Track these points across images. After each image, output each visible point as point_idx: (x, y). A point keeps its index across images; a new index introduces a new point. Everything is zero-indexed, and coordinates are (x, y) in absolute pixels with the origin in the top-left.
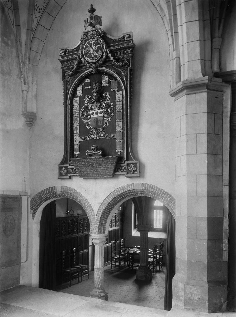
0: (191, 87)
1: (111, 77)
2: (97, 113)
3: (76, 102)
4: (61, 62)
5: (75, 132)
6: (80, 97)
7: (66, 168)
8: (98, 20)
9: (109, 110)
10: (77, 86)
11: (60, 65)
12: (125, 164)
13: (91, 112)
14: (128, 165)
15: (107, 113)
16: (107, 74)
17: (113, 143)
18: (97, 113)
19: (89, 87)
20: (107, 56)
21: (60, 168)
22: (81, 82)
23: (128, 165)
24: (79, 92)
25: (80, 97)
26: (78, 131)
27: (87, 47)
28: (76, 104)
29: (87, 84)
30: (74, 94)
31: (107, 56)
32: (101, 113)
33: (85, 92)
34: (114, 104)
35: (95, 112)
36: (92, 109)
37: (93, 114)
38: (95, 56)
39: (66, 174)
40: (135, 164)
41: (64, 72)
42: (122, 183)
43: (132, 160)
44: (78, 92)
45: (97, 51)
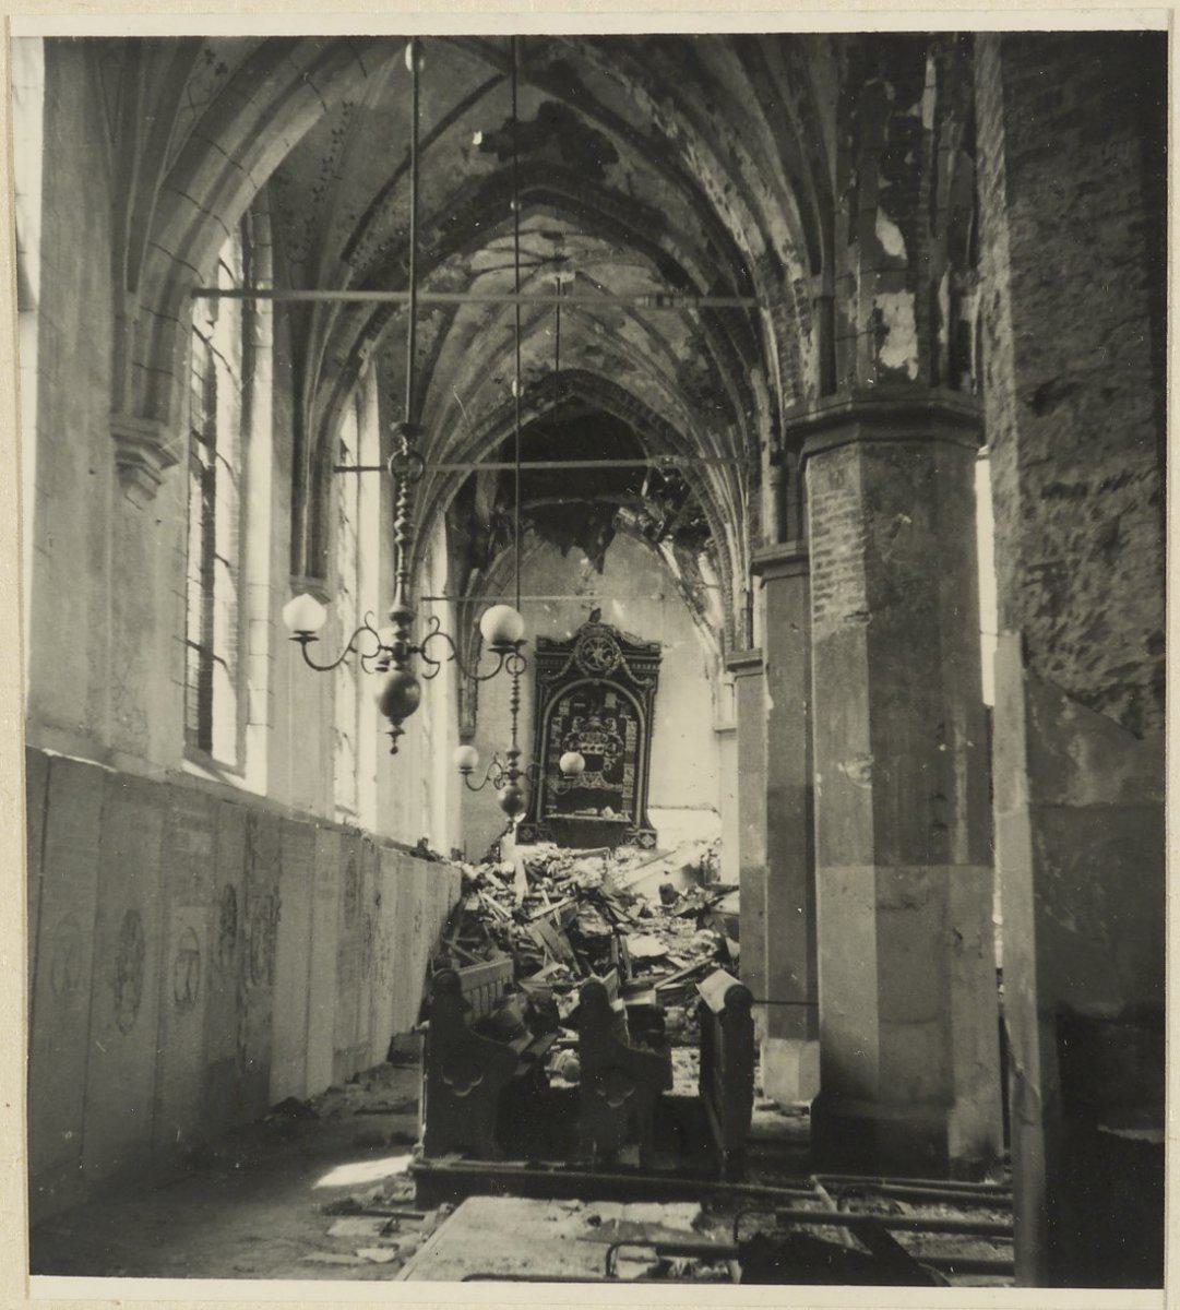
0: (721, 734)
1: (621, 696)
2: (593, 748)
3: (557, 723)
9: (614, 746)
10: (561, 699)
12: (638, 834)
13: (583, 745)
14: (643, 835)
16: (614, 690)
18: (593, 748)
19: (583, 705)
20: (621, 666)
24: (564, 710)
27: (588, 646)
28: (556, 728)
30: (555, 712)
31: (621, 666)
32: (600, 749)
33: (574, 712)
35: (590, 746)
36: (584, 740)
37: (586, 748)
38: (601, 663)
44: (561, 709)
45: (605, 657)
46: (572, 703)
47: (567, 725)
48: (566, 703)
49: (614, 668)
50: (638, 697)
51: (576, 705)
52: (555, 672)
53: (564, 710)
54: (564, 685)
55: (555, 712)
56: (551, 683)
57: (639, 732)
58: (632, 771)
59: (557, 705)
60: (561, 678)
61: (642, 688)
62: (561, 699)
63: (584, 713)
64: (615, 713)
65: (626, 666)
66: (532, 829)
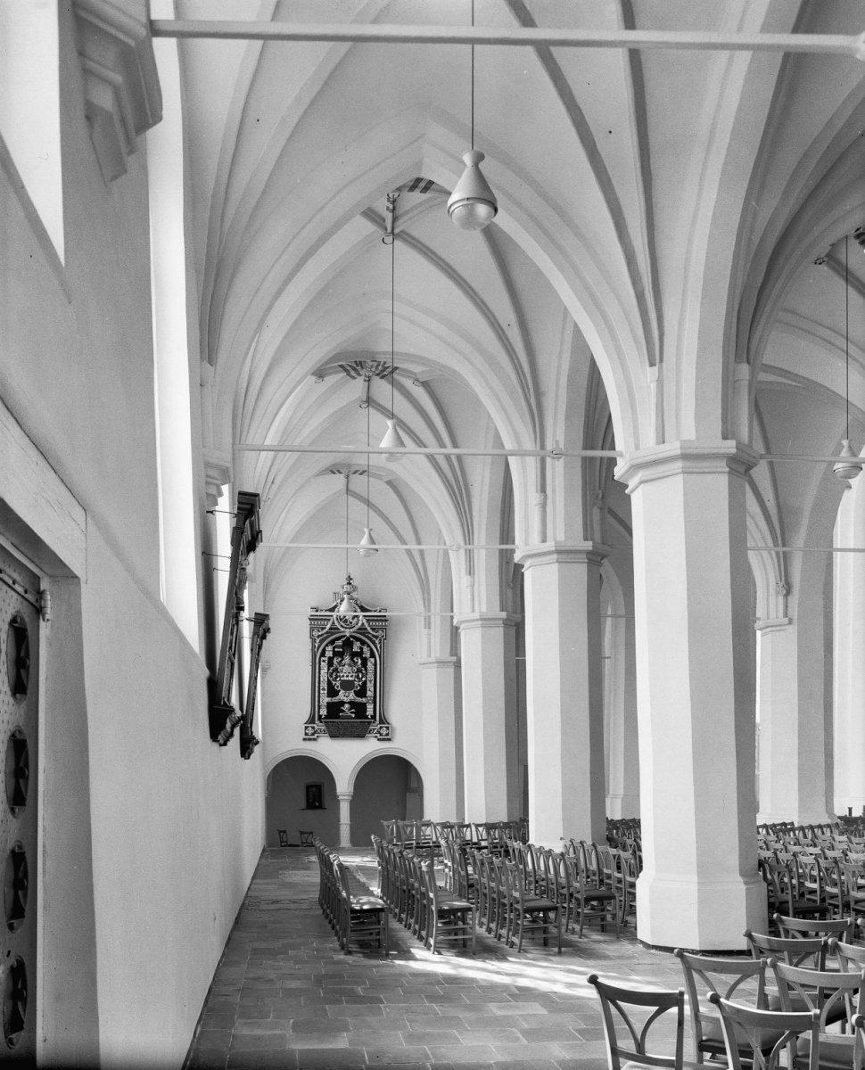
1: (363, 643)
2: (347, 676)
3: (324, 661)
4: (310, 619)
5: (322, 692)
6: (330, 658)
7: (313, 728)
8: (355, 589)
10: (327, 645)
11: (309, 622)
14: (381, 728)
15: (357, 677)
17: (364, 706)
21: (306, 728)
22: (332, 642)
23: (381, 728)
25: (330, 658)
26: (326, 692)
29: (338, 646)
30: (323, 654)
34: (366, 670)
38: (351, 623)
39: (313, 734)
40: (388, 728)
41: (312, 630)
42: (369, 747)
43: (384, 723)
46: (334, 648)
47: (331, 660)
48: (330, 648)
49: (360, 624)
50: (374, 643)
51: (336, 650)
52: (323, 629)
53: (329, 654)
54: (328, 637)
55: (323, 654)
56: (319, 636)
57: (375, 665)
58: (372, 689)
59: (324, 651)
60: (327, 633)
61: (376, 637)
62: (327, 645)
63: (341, 655)
64: (360, 654)
65: (366, 625)
66: (313, 728)
